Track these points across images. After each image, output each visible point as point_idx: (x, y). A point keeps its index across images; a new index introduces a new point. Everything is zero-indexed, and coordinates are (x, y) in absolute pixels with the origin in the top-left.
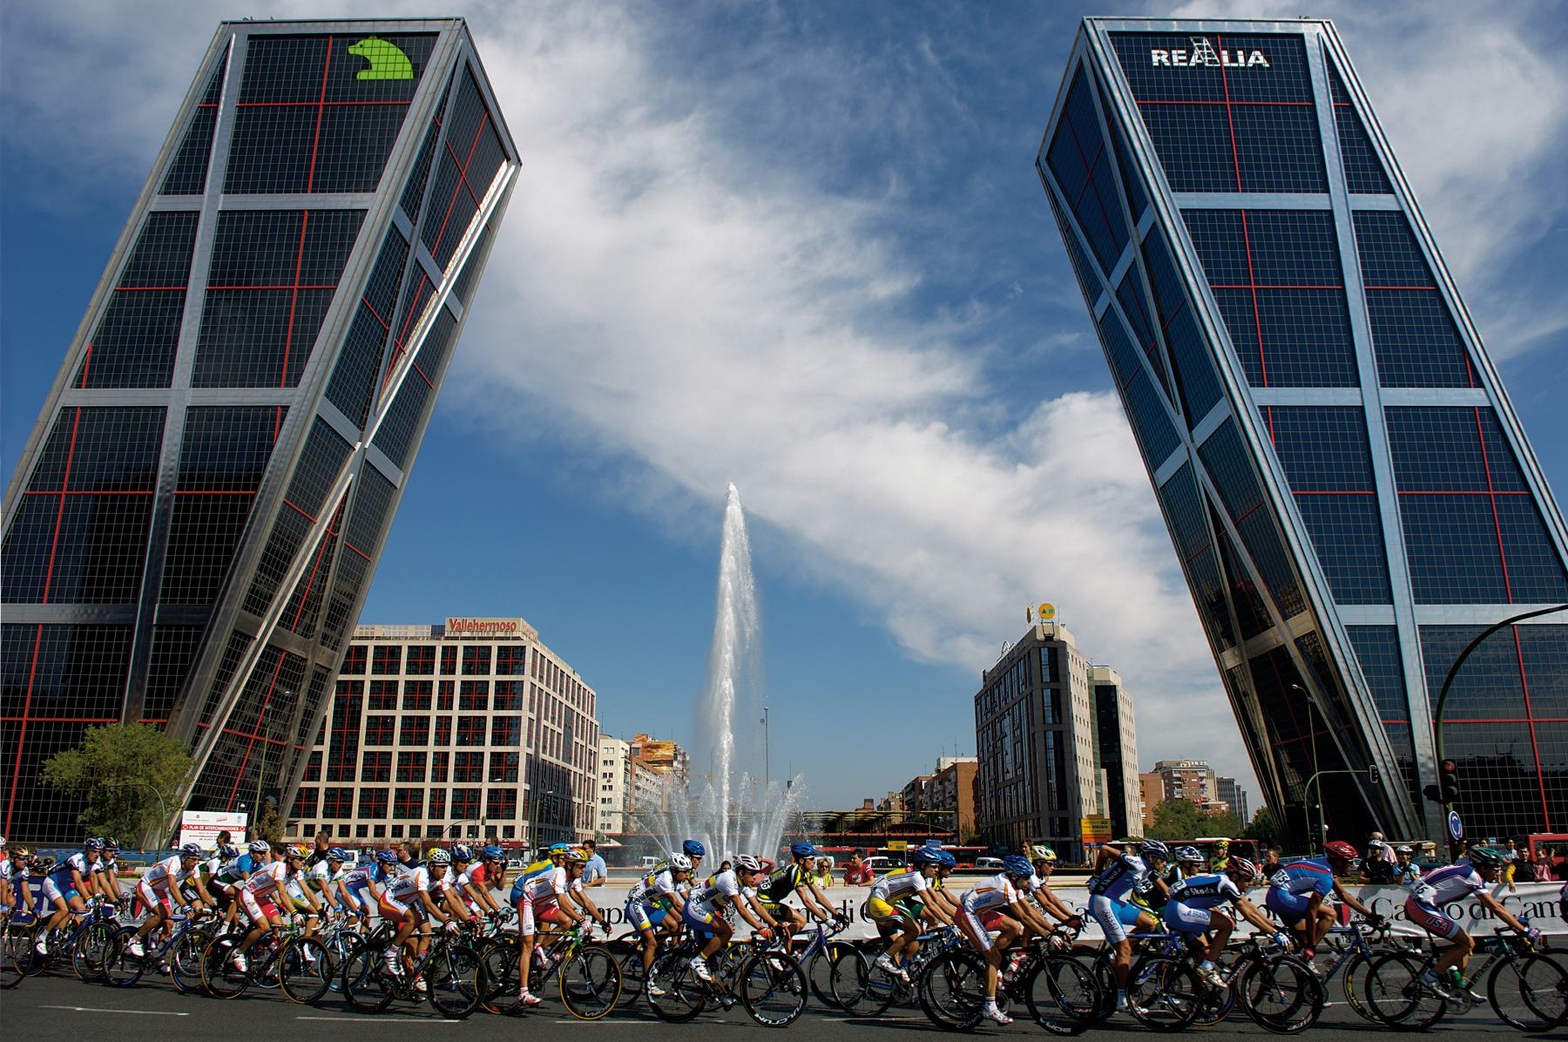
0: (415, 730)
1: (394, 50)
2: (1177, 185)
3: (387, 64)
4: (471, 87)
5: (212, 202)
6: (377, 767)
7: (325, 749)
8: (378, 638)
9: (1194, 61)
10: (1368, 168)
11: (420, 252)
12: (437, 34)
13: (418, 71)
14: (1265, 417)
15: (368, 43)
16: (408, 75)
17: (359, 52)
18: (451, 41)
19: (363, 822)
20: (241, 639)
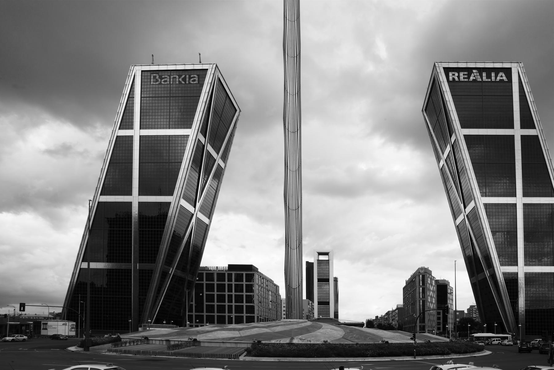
2: (463, 126)
4: (220, 86)
9: (472, 78)
10: (527, 122)
11: (209, 148)
12: (207, 69)
14: (486, 209)
18: (213, 72)
20: (164, 275)
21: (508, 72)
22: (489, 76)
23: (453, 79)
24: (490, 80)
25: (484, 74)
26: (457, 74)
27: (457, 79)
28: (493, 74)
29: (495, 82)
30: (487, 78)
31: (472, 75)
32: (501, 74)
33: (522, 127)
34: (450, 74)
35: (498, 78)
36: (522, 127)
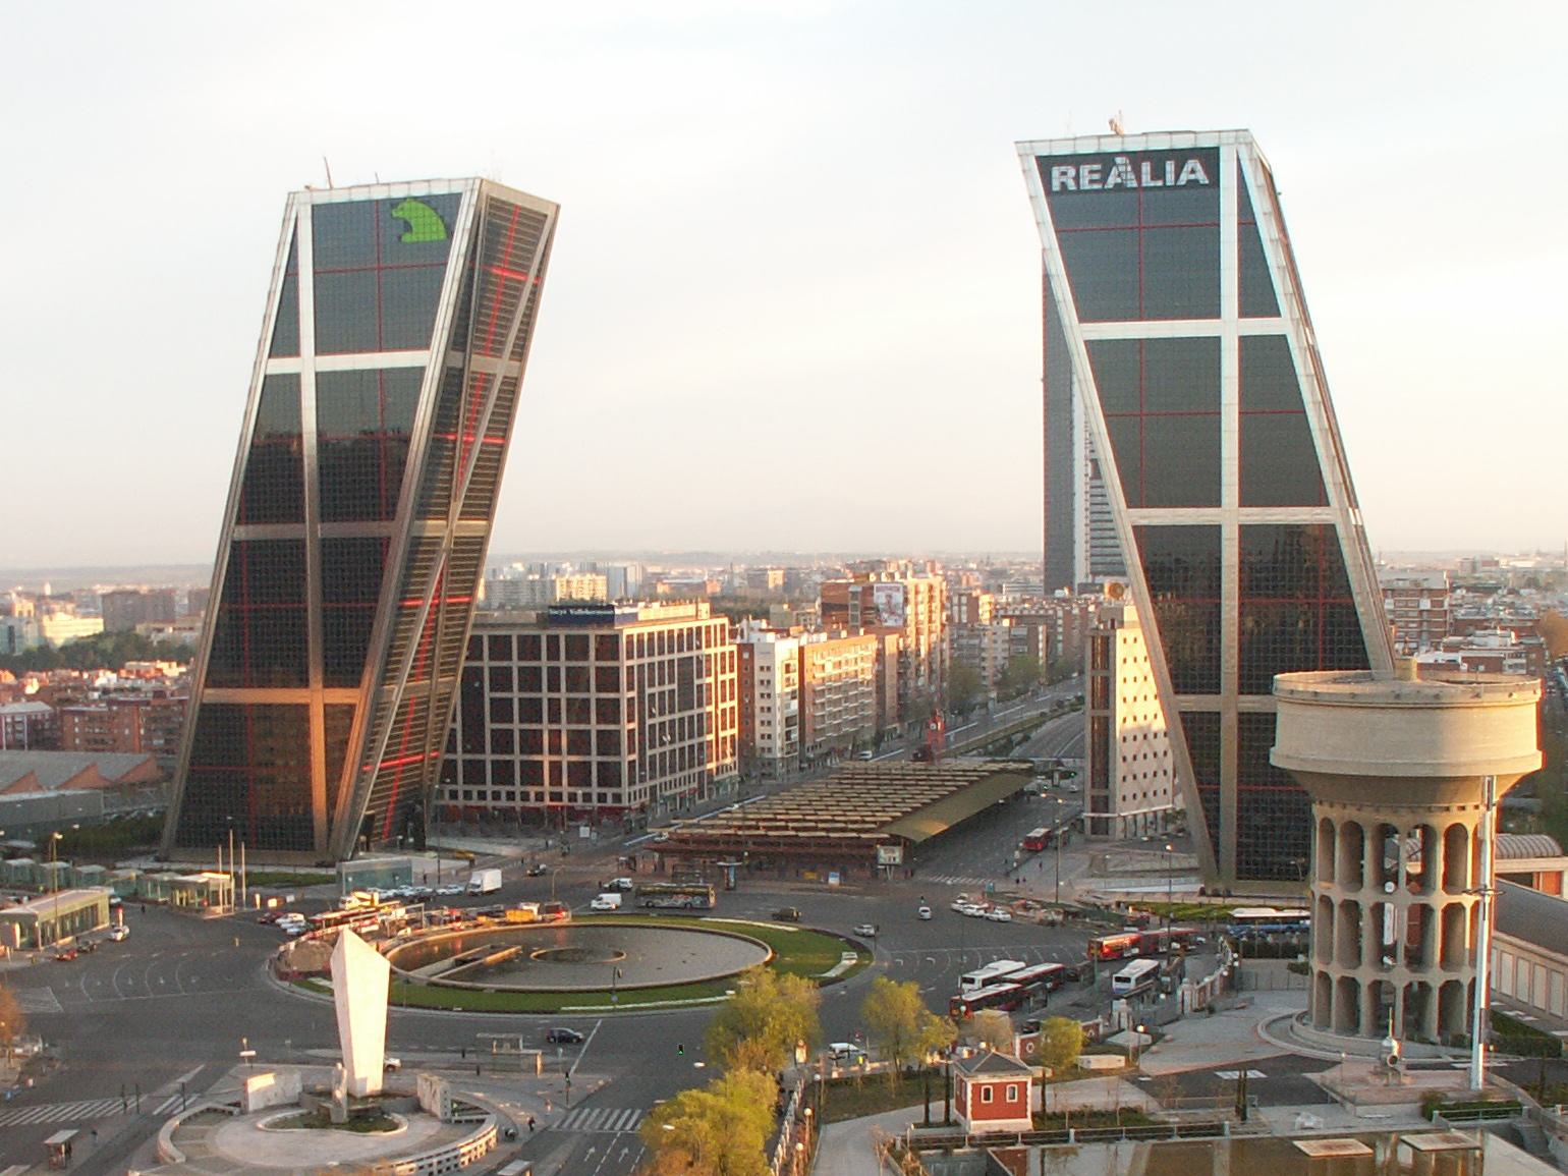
0: (531, 711)
1: (428, 212)
3: (426, 228)
5: (307, 364)
6: (503, 742)
7: (458, 726)
8: (493, 626)
9: (1112, 181)
10: (1258, 298)
13: (450, 233)
15: (406, 205)
16: (442, 236)
17: (400, 214)
19: (496, 788)
21: (1210, 157)
22: (1157, 173)
23: (1063, 185)
24: (1160, 183)
25: (1146, 167)
26: (1072, 172)
27: (1072, 186)
28: (1170, 166)
29: (1175, 187)
30: (1152, 179)
31: (1114, 169)
32: (1191, 164)
33: (1245, 312)
34: (1056, 171)
35: (1184, 178)
36: (1245, 312)
